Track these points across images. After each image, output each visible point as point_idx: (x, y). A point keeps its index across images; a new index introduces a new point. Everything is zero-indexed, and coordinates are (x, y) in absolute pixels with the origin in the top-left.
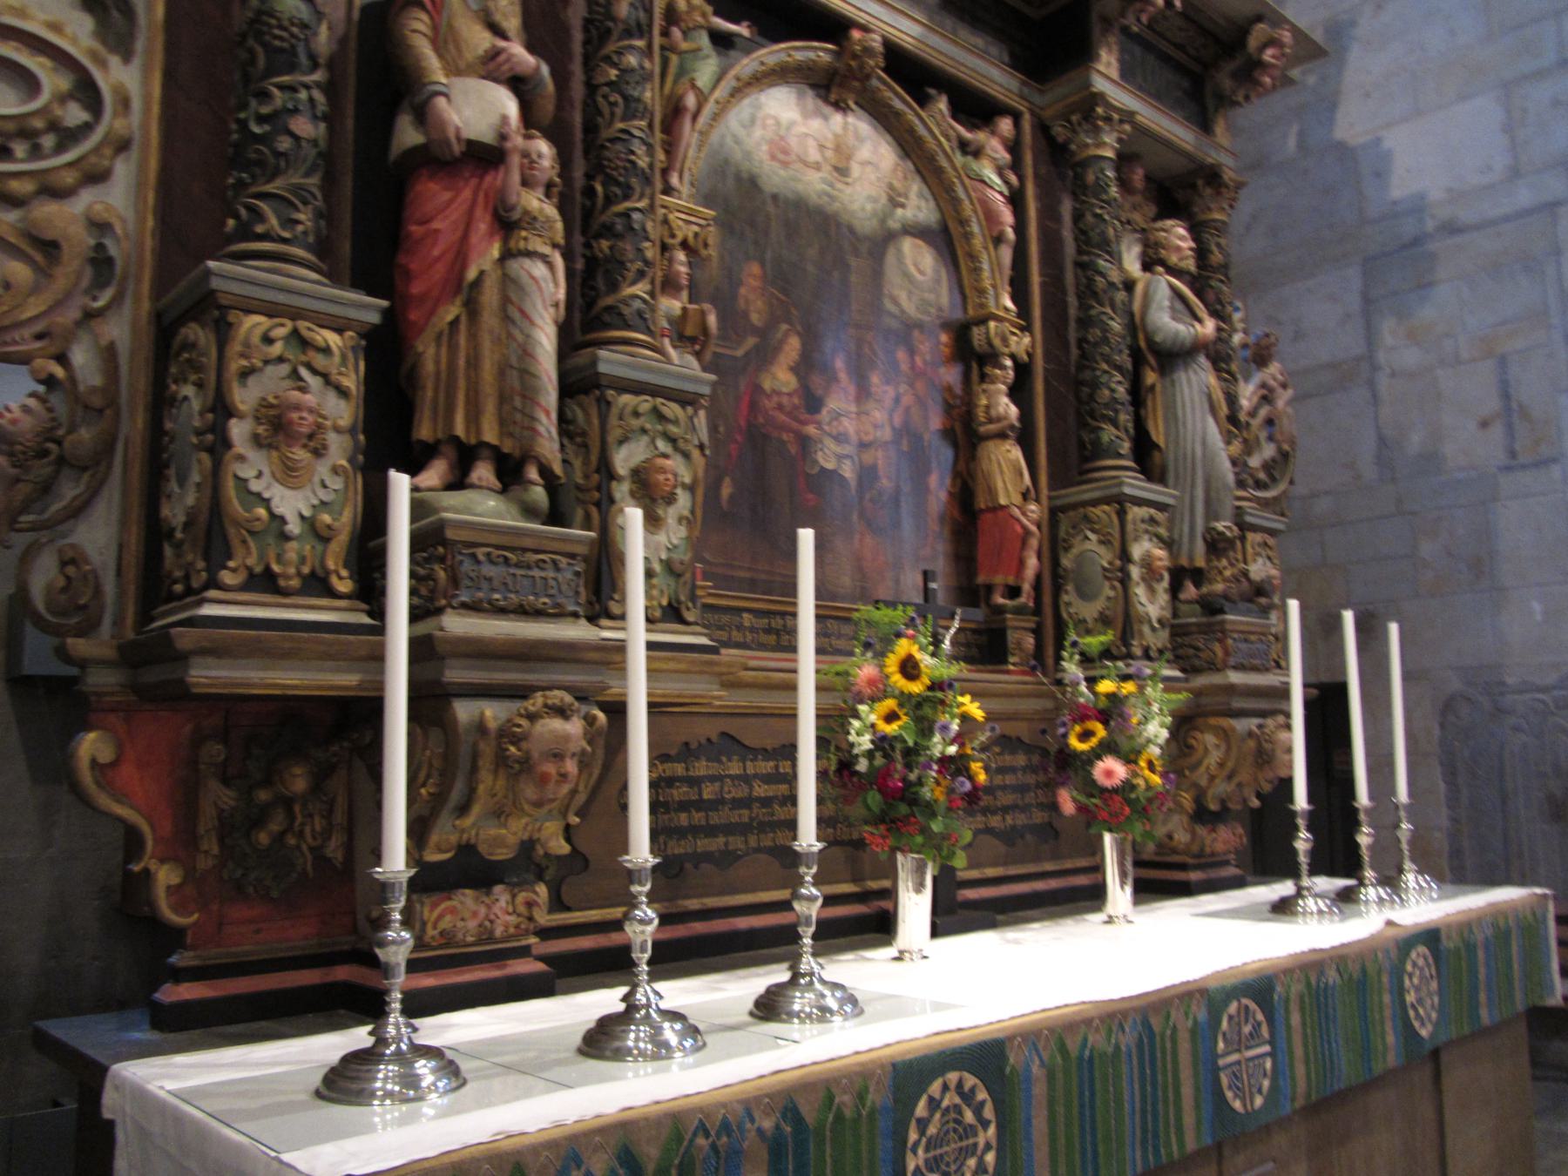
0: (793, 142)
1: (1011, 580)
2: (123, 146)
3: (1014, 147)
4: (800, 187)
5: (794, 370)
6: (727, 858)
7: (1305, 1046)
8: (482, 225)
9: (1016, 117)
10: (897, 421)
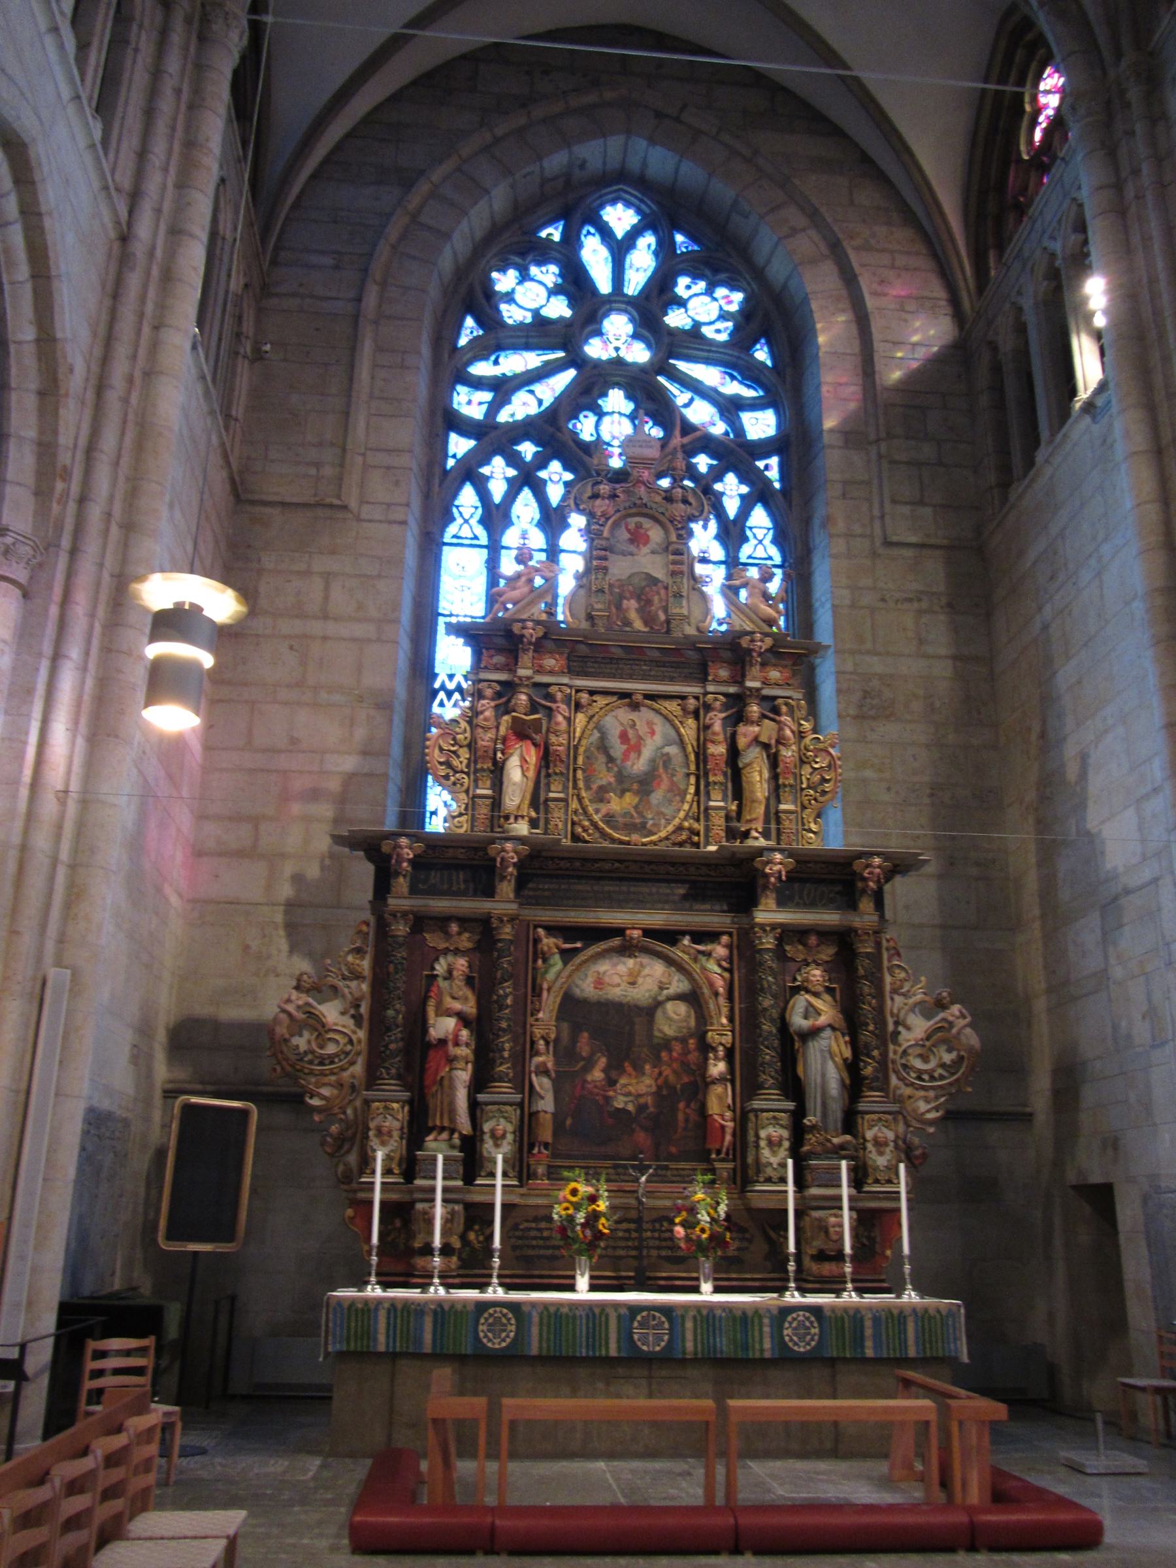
0: (607, 979)
1: (718, 1147)
2: (358, 1054)
3: (729, 947)
4: (610, 997)
5: (604, 1071)
6: (553, 1258)
7: (695, 1340)
8: (443, 1062)
9: (730, 934)
10: (660, 1081)
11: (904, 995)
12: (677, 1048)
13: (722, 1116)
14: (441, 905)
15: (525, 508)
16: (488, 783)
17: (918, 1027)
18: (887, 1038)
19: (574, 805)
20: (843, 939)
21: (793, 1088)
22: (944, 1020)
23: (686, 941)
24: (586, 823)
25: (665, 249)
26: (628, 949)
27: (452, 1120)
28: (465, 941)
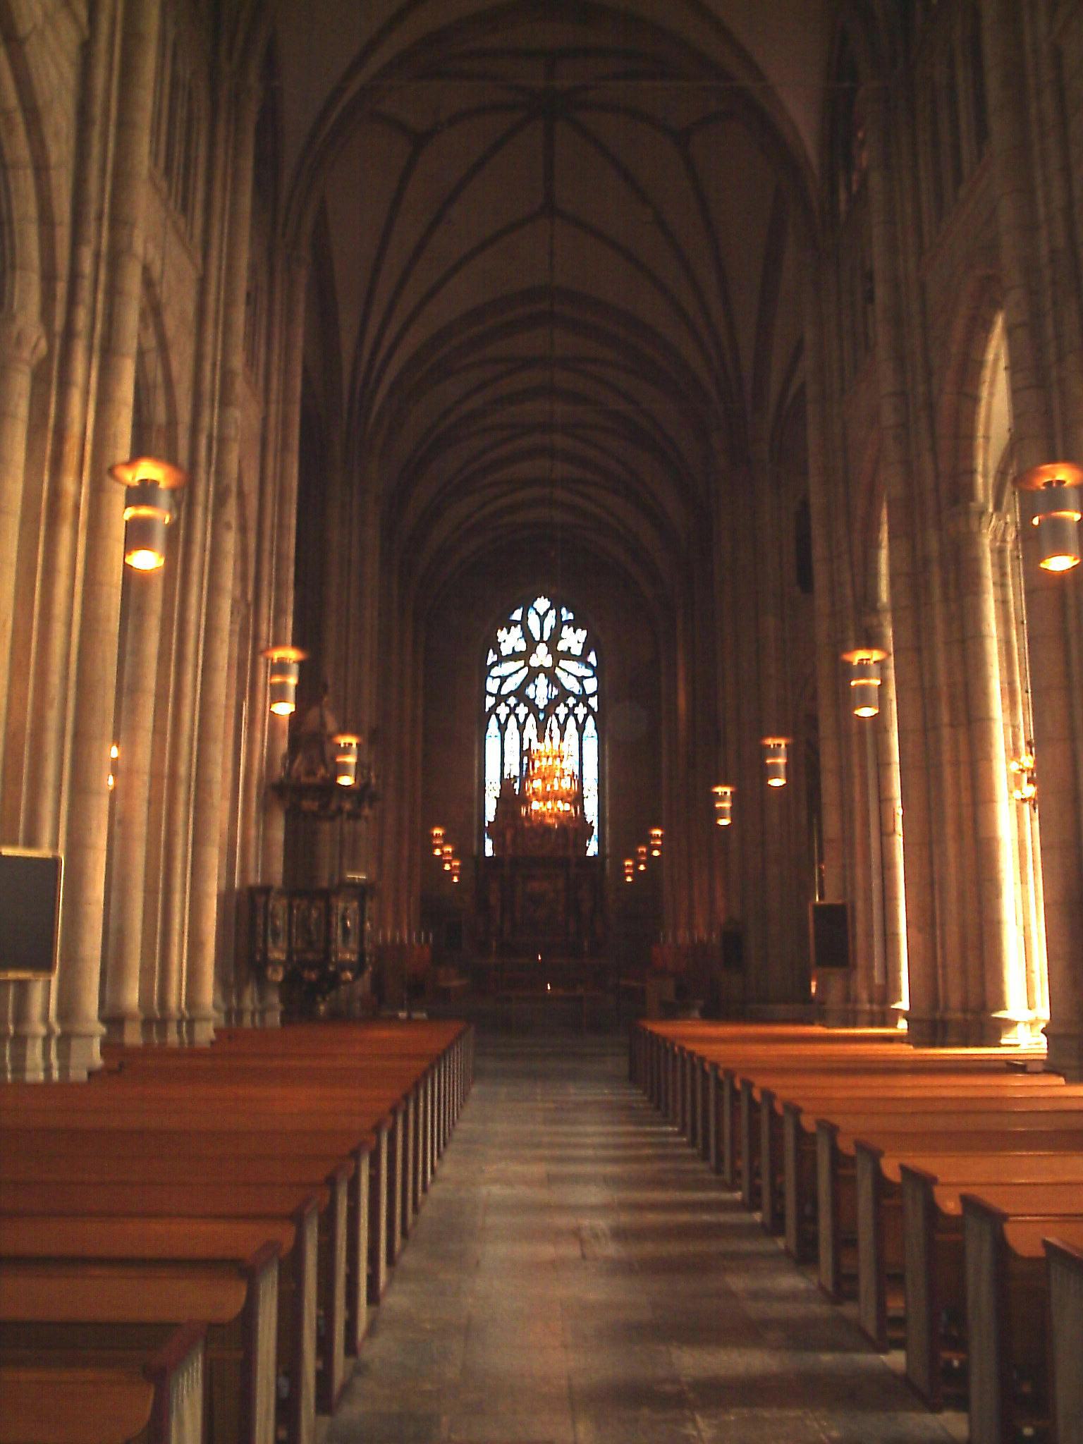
15: (512, 722)
25: (558, 616)
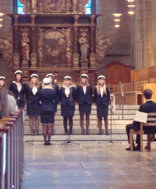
3: (70, 30)
5: (50, 50)
9: (70, 27)
11: (99, 37)
12: (62, 46)
13: (69, 57)
14: (23, 25)
16: (29, 3)
17: (101, 42)
18: (95, 44)
19: (44, 6)
20: (89, 28)
21: (80, 52)
22: (106, 41)
23: (63, 29)
24: (46, 9)
26: (54, 30)
27: (26, 58)
28: (27, 30)
